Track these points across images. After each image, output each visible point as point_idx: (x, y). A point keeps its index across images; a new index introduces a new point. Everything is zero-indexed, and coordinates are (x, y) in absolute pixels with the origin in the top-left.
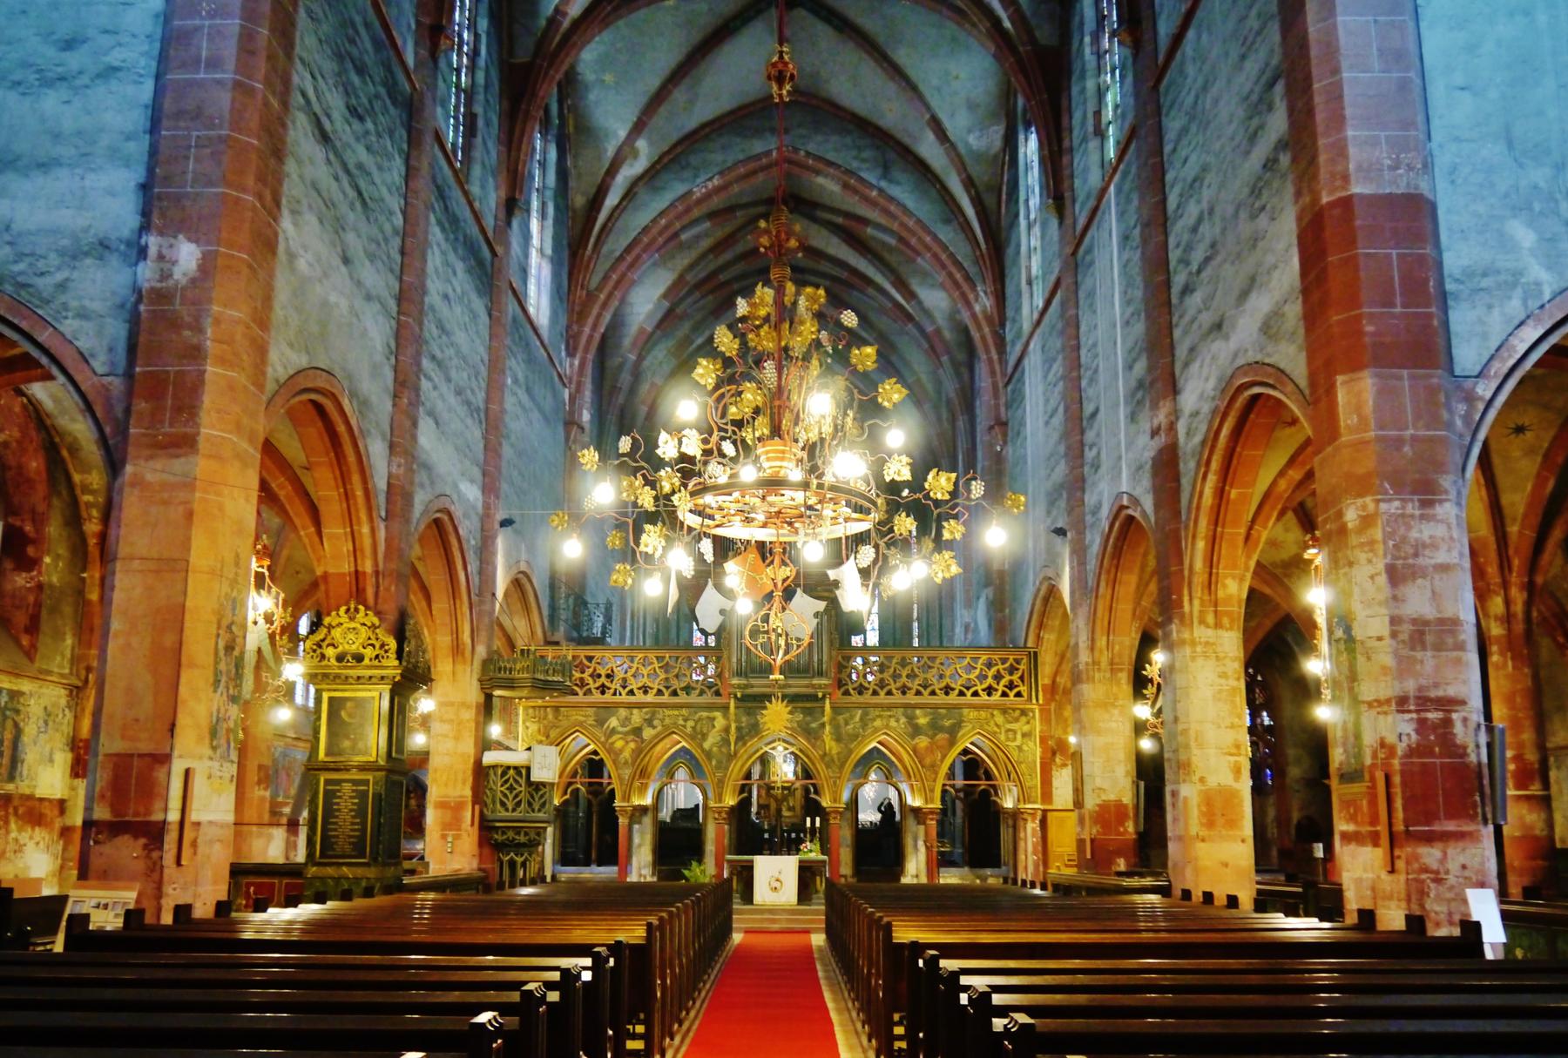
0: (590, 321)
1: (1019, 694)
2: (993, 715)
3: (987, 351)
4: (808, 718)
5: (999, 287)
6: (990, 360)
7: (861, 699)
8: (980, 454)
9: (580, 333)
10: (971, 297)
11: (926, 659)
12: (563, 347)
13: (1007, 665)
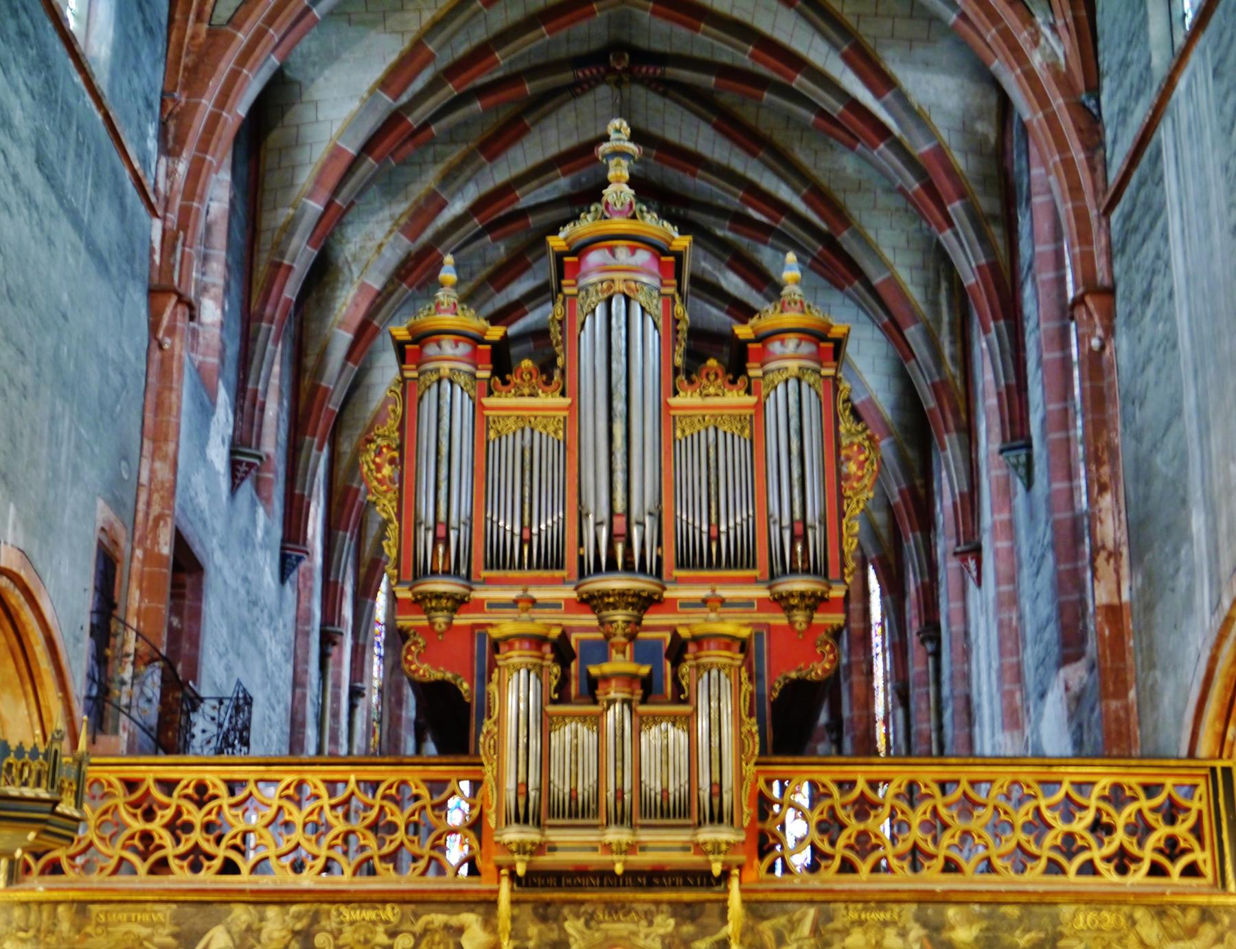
0: (215, 85)
1: (1192, 870)
2: (1133, 922)
3: (1062, 146)
4: (688, 929)
5: (1083, 13)
6: (1068, 165)
7: (814, 882)
8: (1035, 393)
9: (191, 109)
10: (1023, 37)
11: (964, 785)
12: (152, 130)
13: (1159, 800)
